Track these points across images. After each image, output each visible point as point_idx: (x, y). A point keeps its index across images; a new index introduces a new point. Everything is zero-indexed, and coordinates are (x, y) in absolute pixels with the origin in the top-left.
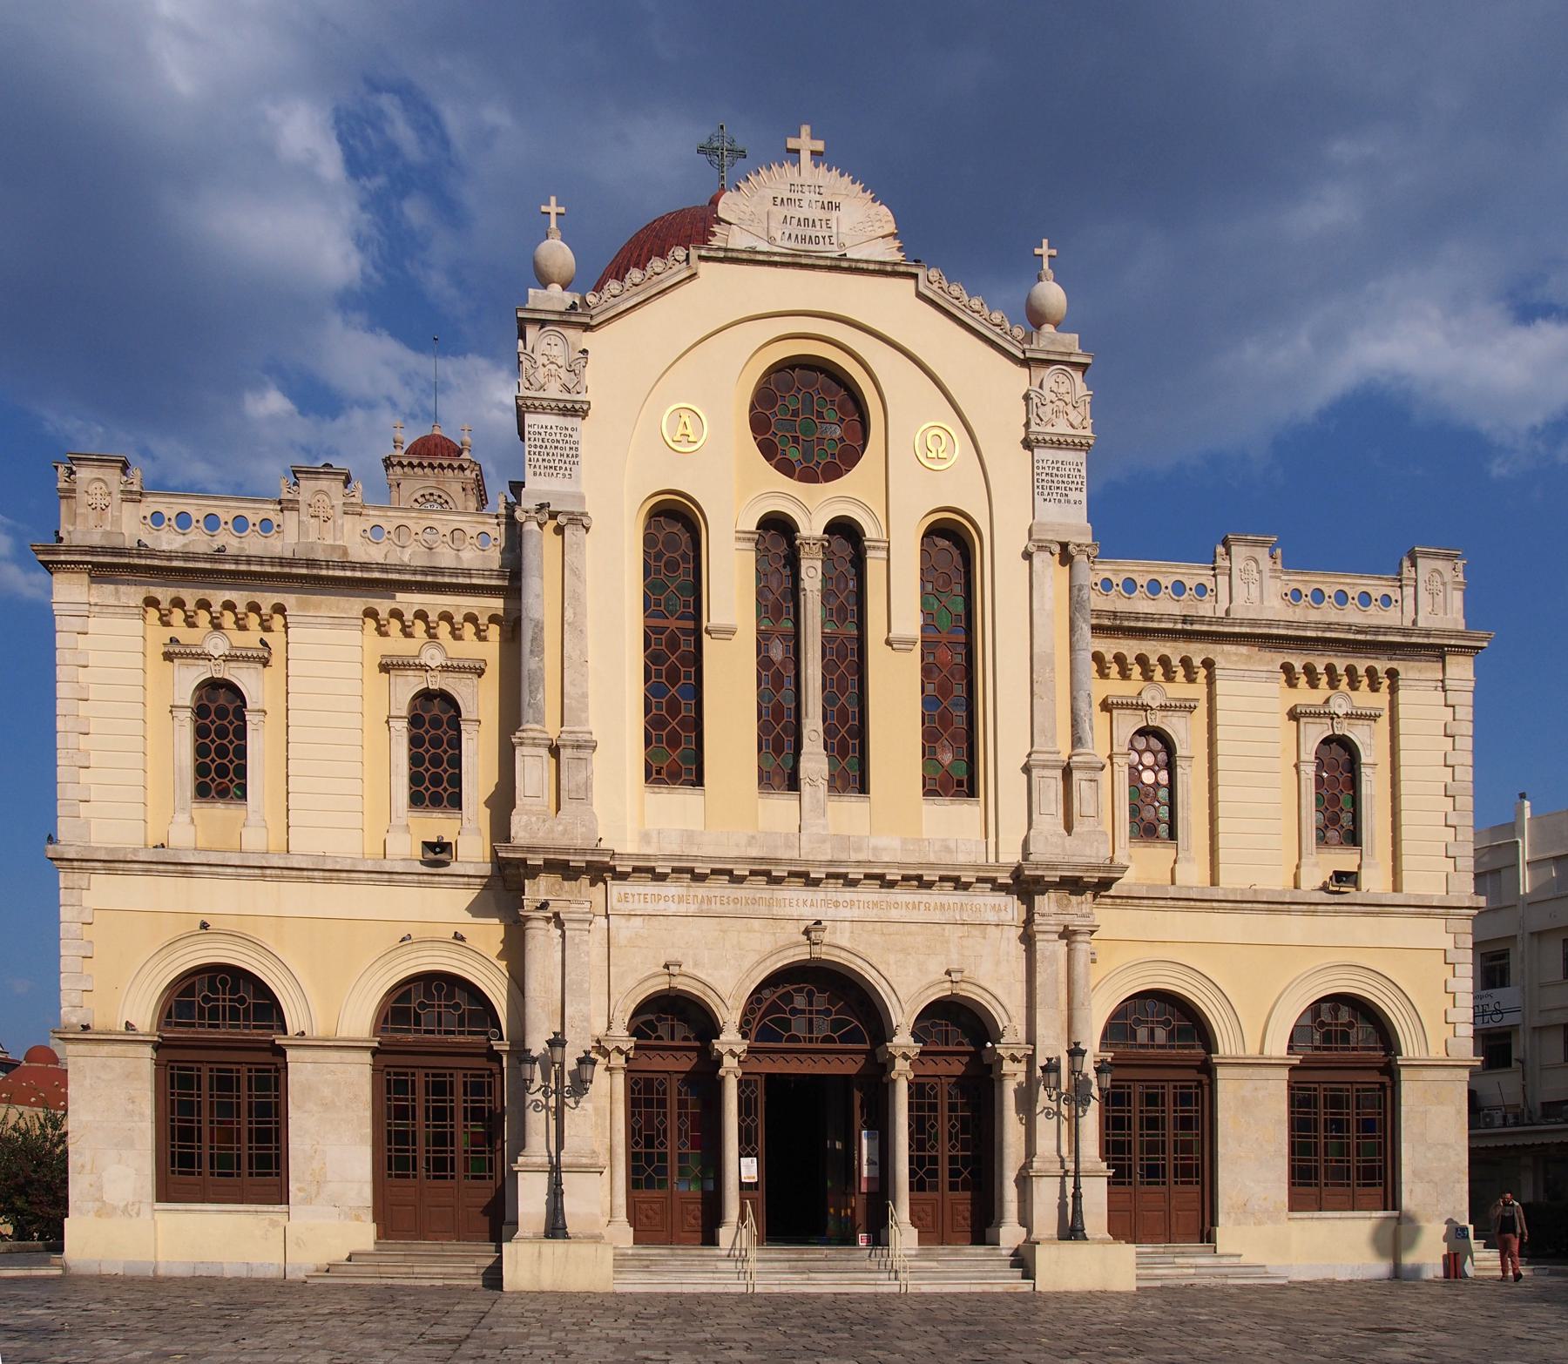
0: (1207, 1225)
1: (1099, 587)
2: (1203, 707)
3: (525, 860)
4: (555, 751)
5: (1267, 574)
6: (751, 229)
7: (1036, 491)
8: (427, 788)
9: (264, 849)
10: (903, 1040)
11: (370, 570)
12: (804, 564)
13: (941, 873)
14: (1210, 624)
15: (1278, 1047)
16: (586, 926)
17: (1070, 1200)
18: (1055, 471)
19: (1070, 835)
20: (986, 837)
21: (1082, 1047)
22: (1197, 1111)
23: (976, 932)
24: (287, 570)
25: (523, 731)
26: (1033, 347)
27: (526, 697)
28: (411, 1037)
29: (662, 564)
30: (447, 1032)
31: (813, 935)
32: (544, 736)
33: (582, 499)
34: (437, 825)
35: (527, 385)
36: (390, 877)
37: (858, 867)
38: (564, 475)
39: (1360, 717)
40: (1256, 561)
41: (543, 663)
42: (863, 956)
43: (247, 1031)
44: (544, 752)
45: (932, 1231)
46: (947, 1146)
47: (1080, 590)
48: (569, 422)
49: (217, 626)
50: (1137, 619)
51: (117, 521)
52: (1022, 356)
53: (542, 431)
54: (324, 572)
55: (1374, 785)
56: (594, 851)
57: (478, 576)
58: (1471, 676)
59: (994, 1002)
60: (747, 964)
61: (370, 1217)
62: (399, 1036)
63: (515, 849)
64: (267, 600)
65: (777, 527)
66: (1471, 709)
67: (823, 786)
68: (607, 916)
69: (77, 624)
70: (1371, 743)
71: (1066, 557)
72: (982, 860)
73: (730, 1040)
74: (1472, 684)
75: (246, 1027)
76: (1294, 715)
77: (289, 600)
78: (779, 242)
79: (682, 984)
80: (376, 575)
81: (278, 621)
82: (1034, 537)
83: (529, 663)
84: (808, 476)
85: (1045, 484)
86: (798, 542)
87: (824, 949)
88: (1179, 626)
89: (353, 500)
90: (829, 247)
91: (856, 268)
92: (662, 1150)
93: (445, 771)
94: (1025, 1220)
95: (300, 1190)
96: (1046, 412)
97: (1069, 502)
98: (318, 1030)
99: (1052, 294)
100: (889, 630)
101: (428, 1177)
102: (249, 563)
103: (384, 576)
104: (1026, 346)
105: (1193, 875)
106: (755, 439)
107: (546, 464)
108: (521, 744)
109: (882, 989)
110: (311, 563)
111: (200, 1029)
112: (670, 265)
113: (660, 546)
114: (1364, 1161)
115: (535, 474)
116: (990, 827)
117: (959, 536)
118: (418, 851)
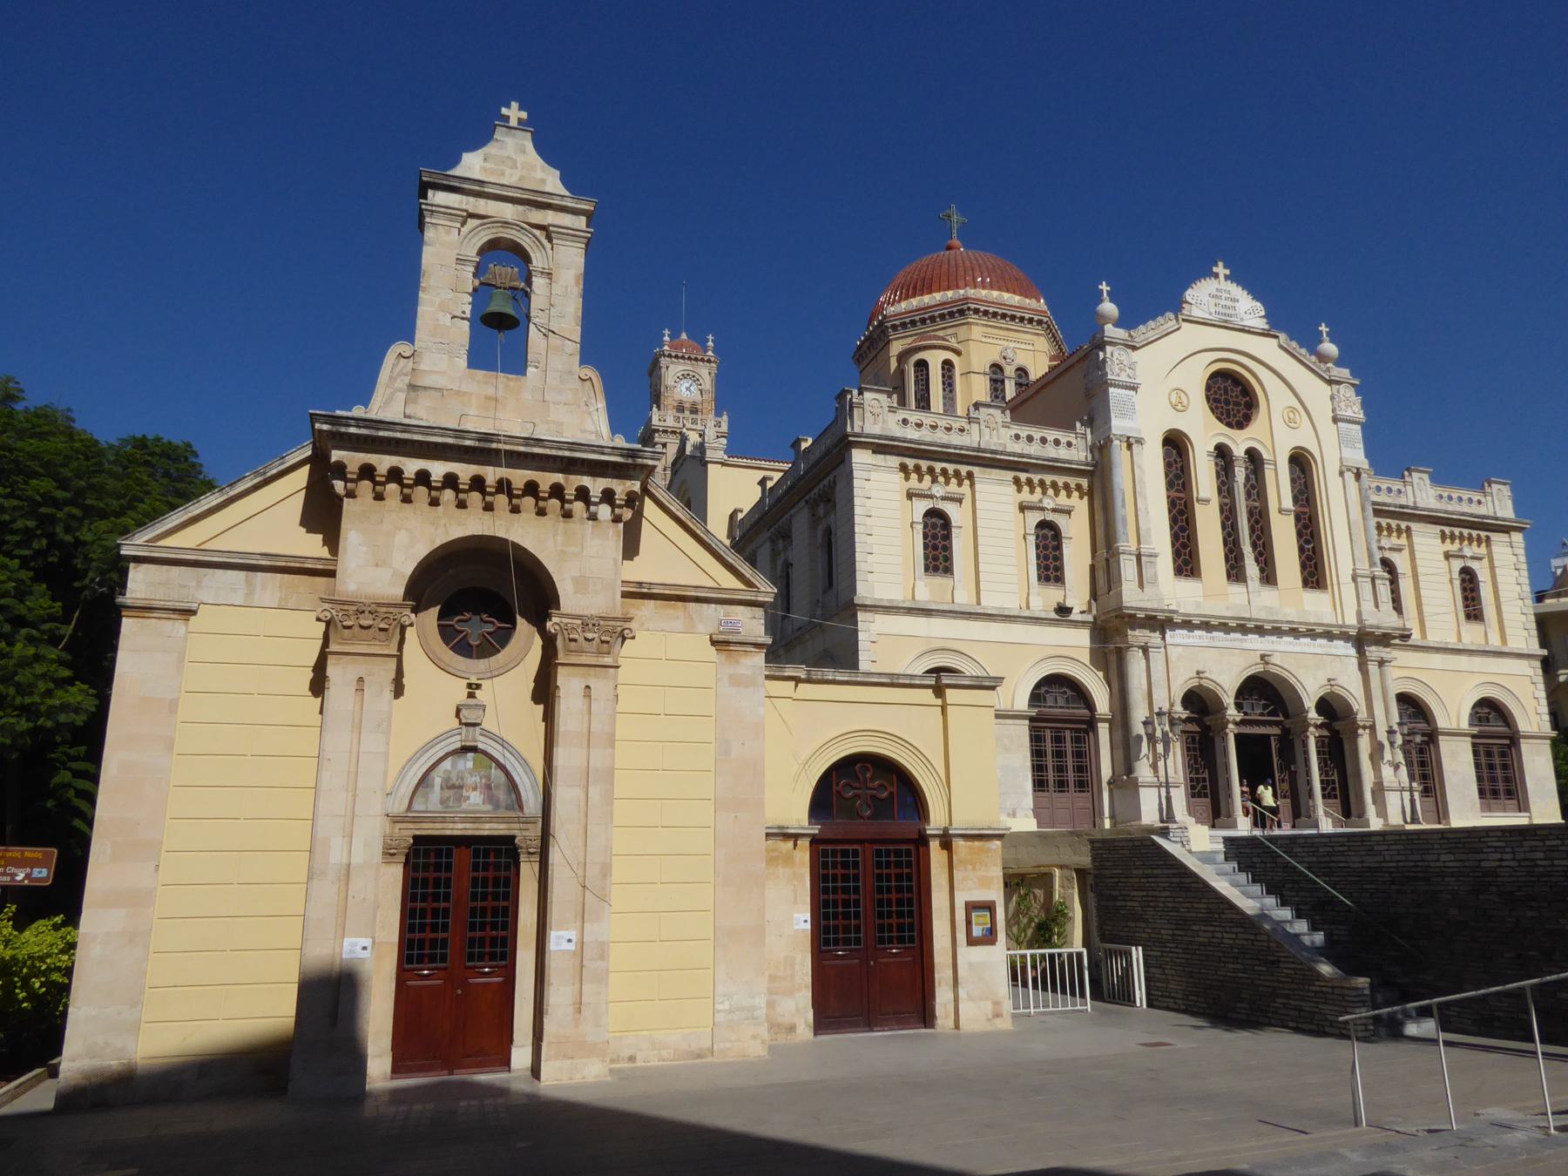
64: (964, 469)
71: (1358, 476)
77: (976, 470)
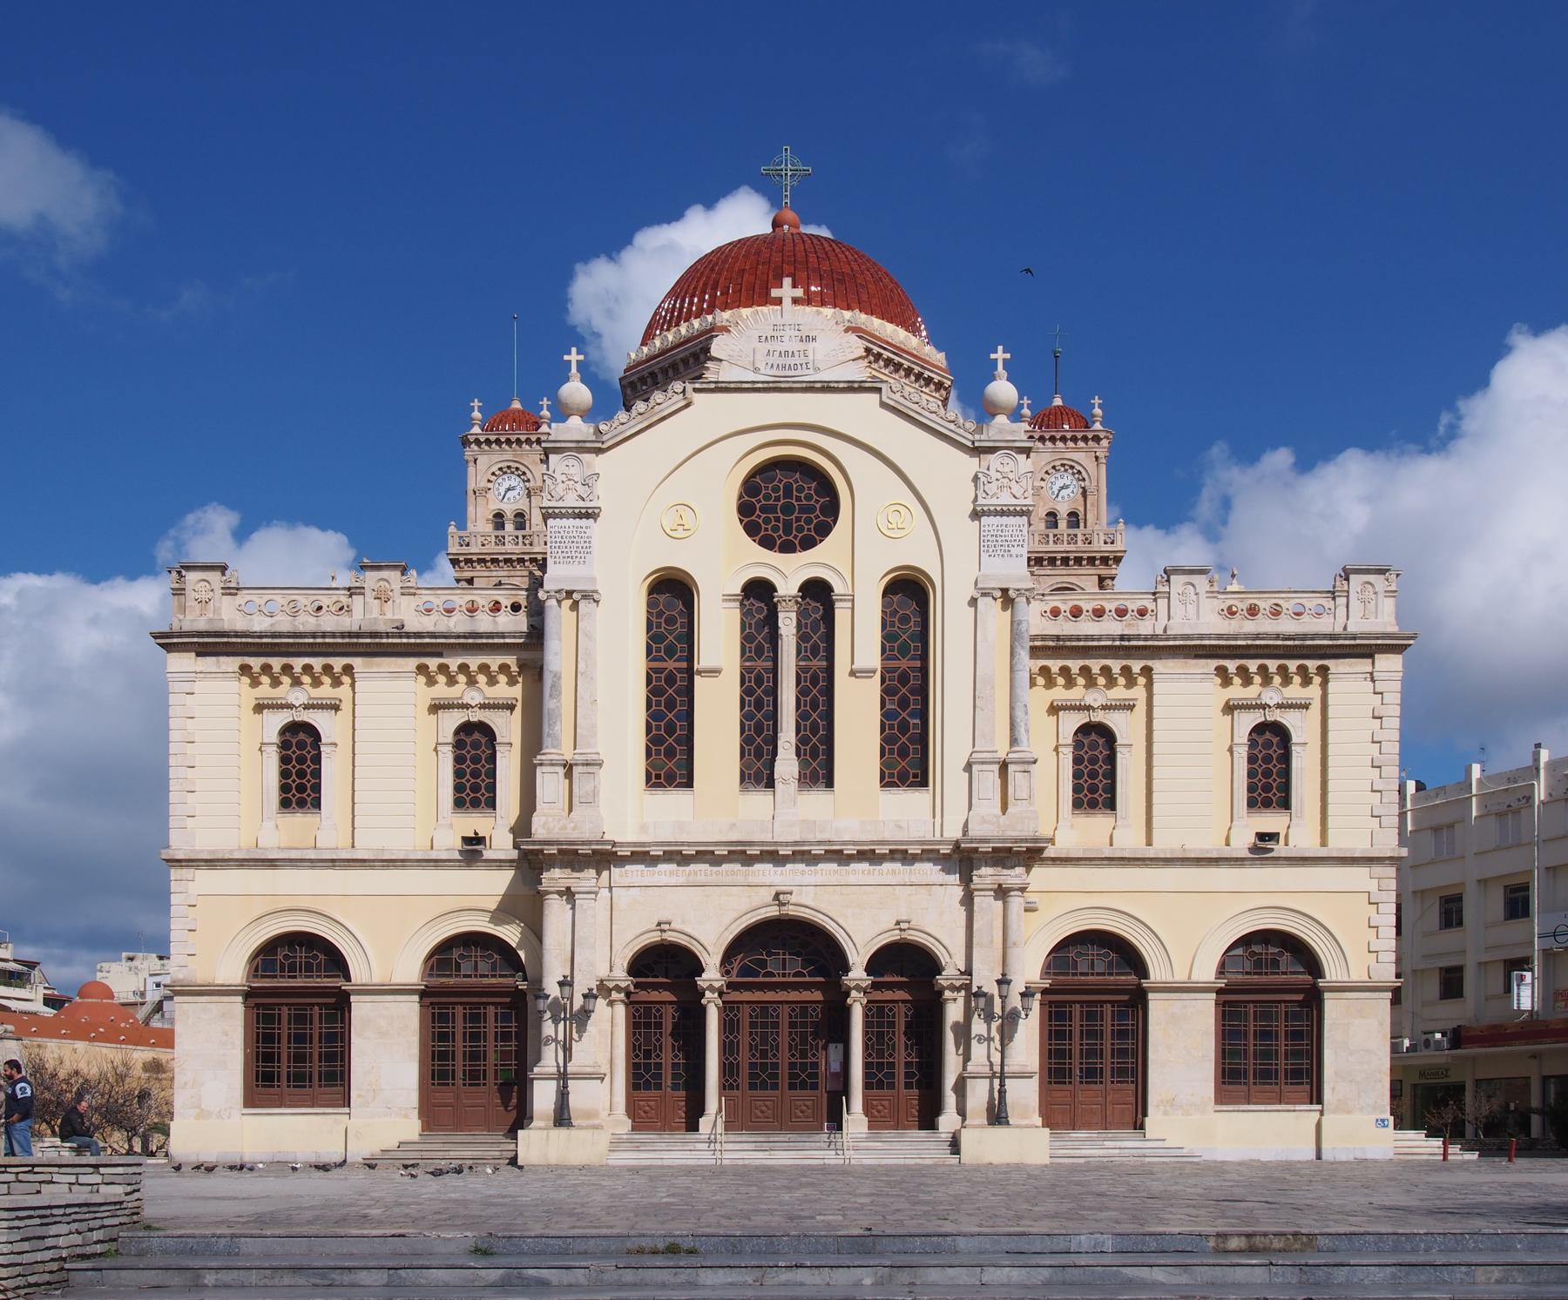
0: (1140, 1116)
1: (1048, 614)
2: (1141, 707)
3: (542, 850)
4: (569, 769)
5: (1203, 595)
6: (739, 363)
7: (982, 549)
8: (468, 795)
9: (334, 846)
10: (857, 974)
11: (423, 637)
12: (781, 616)
13: (891, 847)
14: (1146, 639)
15: (1206, 972)
16: (593, 896)
17: (996, 1095)
18: (999, 533)
19: (1004, 814)
20: (934, 817)
21: (1009, 977)
22: (1133, 1025)
23: (923, 890)
24: (355, 640)
25: (544, 754)
26: (983, 437)
27: (546, 729)
28: (452, 981)
29: (662, 620)
30: (482, 976)
31: (781, 897)
32: (561, 757)
33: (593, 580)
34: (475, 822)
35: (549, 497)
36: (436, 863)
37: (819, 845)
38: (579, 562)
39: (1291, 706)
40: (1193, 585)
41: (559, 705)
42: (824, 911)
43: (319, 980)
44: (561, 771)
45: (878, 1119)
46: (903, 1054)
47: (1019, 625)
48: (584, 522)
49: (297, 682)
50: (1079, 640)
51: (217, 611)
52: (969, 444)
53: (561, 530)
54: (384, 641)
55: (1304, 764)
56: (598, 842)
57: (509, 637)
58: (1400, 668)
59: (937, 943)
60: (727, 920)
61: (416, 1112)
62: (443, 980)
63: (534, 843)
64: (338, 663)
65: (758, 592)
66: (1399, 695)
67: (794, 785)
68: (610, 888)
69: (187, 687)
70: (1302, 728)
71: (1007, 599)
72: (929, 837)
73: (712, 975)
74: (1401, 674)
75: (318, 976)
76: (1229, 709)
77: (357, 663)
78: (763, 371)
79: (671, 937)
80: (427, 640)
81: (346, 679)
82: (979, 586)
83: (549, 704)
84: (787, 548)
85: (990, 543)
86: (775, 600)
87: (791, 907)
88: (1117, 643)
89: (409, 584)
90: (807, 372)
91: (827, 388)
92: (658, 1061)
93: (483, 781)
94: (962, 1112)
95: (359, 1096)
96: (992, 489)
97: (1011, 556)
98: (377, 978)
99: (1003, 390)
100: (853, 663)
101: (464, 1085)
102: (323, 637)
103: (433, 641)
104: (977, 437)
105: (1130, 839)
106: (741, 521)
107: (565, 555)
108: (541, 765)
109: (841, 936)
110: (373, 635)
111: (281, 980)
112: (669, 396)
113: (661, 607)
114: (1292, 1064)
115: (555, 563)
116: (937, 810)
117: (919, 584)
118: (458, 844)
